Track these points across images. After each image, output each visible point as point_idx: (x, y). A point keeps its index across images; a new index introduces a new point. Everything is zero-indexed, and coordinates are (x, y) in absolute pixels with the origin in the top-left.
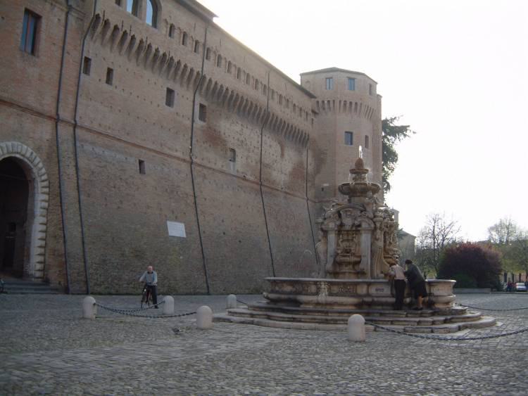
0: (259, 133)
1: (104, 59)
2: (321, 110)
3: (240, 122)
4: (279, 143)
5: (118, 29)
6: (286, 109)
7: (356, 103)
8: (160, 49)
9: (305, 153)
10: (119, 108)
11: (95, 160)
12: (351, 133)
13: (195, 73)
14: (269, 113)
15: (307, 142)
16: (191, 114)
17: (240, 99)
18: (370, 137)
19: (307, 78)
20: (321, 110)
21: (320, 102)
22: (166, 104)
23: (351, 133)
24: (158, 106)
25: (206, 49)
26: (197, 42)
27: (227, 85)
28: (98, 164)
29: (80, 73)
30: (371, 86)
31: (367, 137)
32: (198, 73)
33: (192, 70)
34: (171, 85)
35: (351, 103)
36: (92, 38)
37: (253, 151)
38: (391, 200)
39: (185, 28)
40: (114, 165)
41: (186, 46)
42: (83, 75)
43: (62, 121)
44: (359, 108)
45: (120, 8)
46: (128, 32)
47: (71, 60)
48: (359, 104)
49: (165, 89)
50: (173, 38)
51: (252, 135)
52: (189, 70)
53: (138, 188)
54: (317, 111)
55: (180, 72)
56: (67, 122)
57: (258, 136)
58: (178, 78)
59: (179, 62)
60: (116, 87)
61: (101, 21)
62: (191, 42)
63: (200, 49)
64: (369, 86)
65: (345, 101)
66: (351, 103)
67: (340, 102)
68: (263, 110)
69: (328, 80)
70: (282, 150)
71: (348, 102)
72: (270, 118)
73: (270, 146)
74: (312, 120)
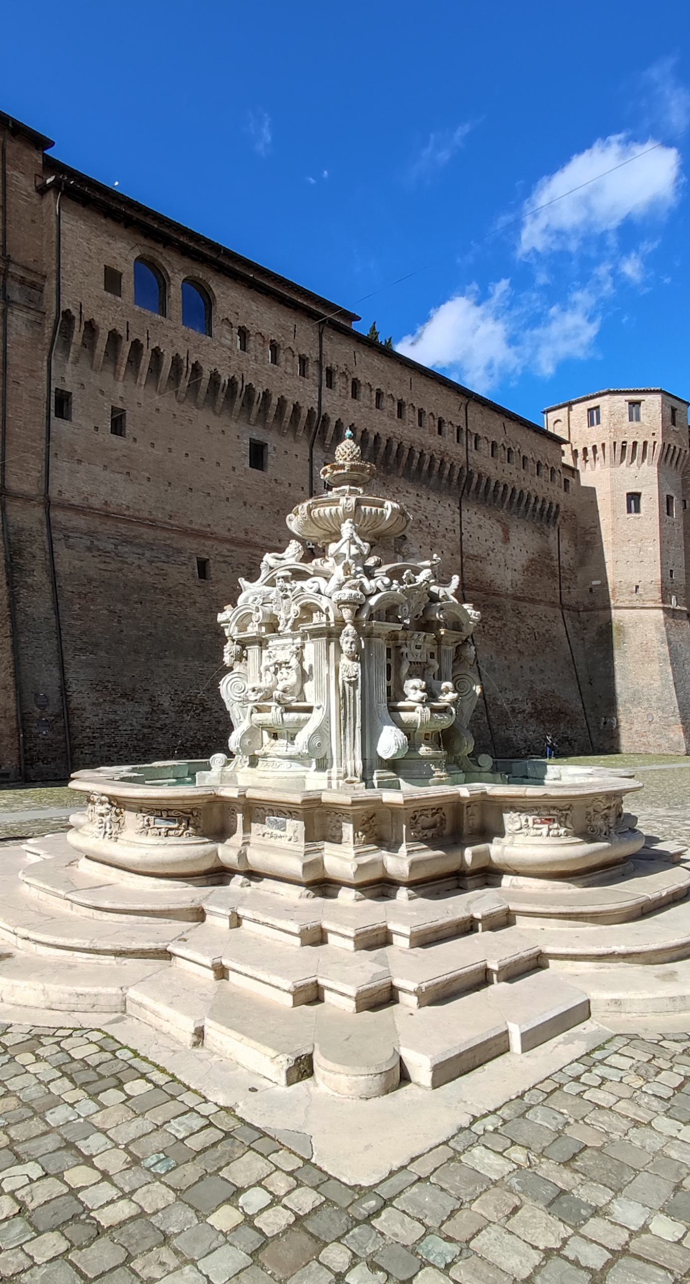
0: (455, 507)
1: (102, 392)
3: (411, 490)
4: (498, 521)
5: (121, 337)
6: (507, 464)
9: (553, 536)
10: (147, 475)
11: (96, 560)
13: (304, 413)
14: (470, 473)
15: (555, 517)
16: (307, 480)
17: (406, 453)
22: (250, 466)
24: (234, 469)
25: (324, 373)
26: (303, 360)
27: (376, 430)
28: (102, 566)
29: (48, 417)
32: (311, 411)
33: (297, 408)
34: (258, 434)
36: (68, 355)
37: (444, 536)
40: (139, 567)
42: (56, 422)
43: (16, 497)
45: (119, 299)
46: (143, 341)
47: (25, 396)
49: (247, 442)
51: (440, 510)
52: (290, 408)
53: (195, 603)
55: (272, 411)
56: (27, 499)
57: (454, 512)
58: (270, 420)
59: (266, 395)
60: (135, 440)
61: (77, 323)
62: (290, 357)
63: (312, 369)
67: (615, 443)
68: (457, 469)
70: (506, 531)
72: (475, 480)
73: (480, 526)
74: (566, 481)
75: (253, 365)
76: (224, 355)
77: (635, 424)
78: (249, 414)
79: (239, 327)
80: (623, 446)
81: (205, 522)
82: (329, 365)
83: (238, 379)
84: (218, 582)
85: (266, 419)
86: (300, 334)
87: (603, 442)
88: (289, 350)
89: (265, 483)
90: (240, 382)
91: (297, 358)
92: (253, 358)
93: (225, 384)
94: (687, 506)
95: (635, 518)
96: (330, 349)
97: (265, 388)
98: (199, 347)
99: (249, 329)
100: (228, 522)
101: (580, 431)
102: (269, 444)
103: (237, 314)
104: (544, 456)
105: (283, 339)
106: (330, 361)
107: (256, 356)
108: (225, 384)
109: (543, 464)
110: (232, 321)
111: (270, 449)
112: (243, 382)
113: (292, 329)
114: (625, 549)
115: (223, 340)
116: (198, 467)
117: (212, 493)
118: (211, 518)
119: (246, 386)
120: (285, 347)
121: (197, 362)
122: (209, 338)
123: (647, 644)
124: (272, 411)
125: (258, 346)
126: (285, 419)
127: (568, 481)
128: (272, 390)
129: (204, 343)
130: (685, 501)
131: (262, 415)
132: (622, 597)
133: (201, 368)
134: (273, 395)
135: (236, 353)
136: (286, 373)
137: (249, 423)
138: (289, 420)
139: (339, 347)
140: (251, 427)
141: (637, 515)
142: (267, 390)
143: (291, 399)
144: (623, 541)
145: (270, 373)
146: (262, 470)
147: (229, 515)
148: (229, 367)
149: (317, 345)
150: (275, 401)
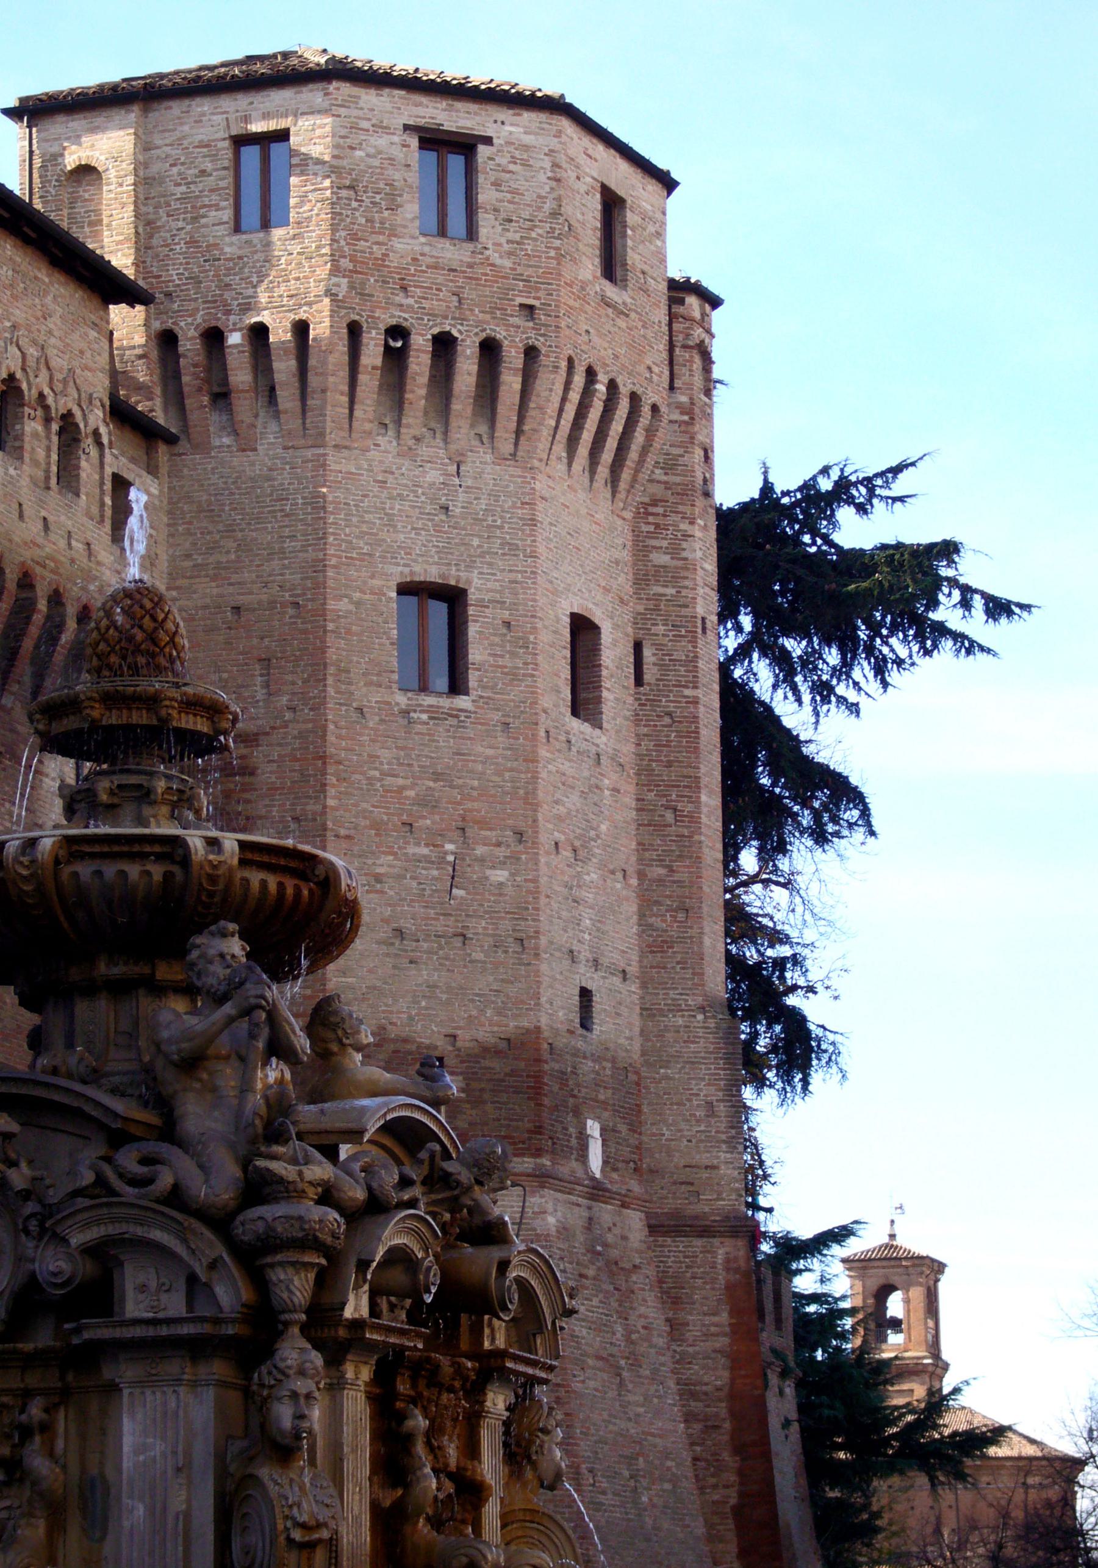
2: (198, 402)
7: (490, 349)
18: (609, 636)
20: (198, 402)
21: (190, 344)
35: (444, 345)
44: (511, 382)
48: (513, 357)
54: (159, 414)
64: (595, 203)
65: (397, 332)
66: (444, 345)
67: (354, 331)
71: (421, 343)
80: (387, 347)
94: (647, 677)
95: (435, 714)
101: (192, 242)
104: (32, 352)
109: (30, 394)
130: (638, 647)
141: (445, 702)
144: (378, 827)
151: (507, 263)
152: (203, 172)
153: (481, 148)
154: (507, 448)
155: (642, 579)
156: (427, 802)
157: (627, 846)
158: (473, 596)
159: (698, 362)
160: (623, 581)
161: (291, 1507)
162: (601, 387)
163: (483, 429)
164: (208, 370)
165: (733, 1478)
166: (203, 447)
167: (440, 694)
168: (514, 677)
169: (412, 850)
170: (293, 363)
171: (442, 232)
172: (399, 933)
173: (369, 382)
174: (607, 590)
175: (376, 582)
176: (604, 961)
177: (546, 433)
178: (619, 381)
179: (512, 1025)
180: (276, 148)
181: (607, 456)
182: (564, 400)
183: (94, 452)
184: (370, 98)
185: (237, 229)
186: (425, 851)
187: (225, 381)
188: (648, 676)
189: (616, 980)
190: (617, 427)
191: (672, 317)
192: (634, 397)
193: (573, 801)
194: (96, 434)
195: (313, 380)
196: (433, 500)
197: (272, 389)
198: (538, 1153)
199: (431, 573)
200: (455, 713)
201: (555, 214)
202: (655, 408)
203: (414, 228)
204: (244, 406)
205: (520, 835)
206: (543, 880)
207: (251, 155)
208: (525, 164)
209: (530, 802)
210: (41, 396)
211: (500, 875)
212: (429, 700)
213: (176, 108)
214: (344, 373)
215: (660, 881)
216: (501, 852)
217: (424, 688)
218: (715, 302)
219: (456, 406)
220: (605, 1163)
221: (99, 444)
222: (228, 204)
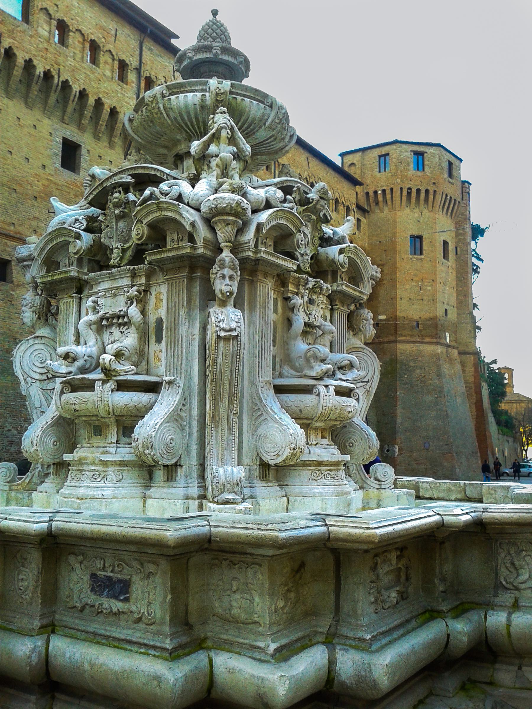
2: (373, 204)
7: (427, 191)
8: (35, 62)
12: (420, 238)
19: (349, 159)
21: (371, 194)
22: (62, 166)
23: (420, 238)
26: (123, 66)
30: (450, 164)
31: (445, 243)
35: (418, 191)
38: (245, 79)
39: (95, 35)
41: (98, 66)
44: (431, 197)
48: (431, 192)
50: (67, 47)
55: (88, 113)
58: (85, 122)
59: (83, 94)
62: (110, 61)
63: (132, 76)
65: (410, 189)
66: (418, 191)
69: (382, 159)
71: (414, 190)
75: (71, 62)
76: (41, 46)
77: (419, 173)
78: (64, 112)
79: (59, 19)
80: (408, 192)
81: (9, 220)
82: (148, 75)
83: (54, 73)
84: (18, 286)
85: (80, 120)
86: (121, 37)
87: (392, 186)
88: (108, 53)
89: (76, 186)
90: (56, 77)
91: (116, 63)
92: (72, 54)
93: (39, 76)
95: (417, 259)
96: (150, 60)
97: (82, 87)
98: (13, 33)
99: (69, 24)
100: (34, 223)
101: (372, 175)
102: (83, 145)
103: (57, 5)
104: (341, 194)
105: (103, 40)
106: (148, 70)
107: (74, 53)
108: (39, 76)
109: (340, 201)
110: (51, 12)
111: (84, 151)
112: (59, 77)
113: (113, 32)
114: (407, 287)
115: (40, 30)
116: (5, 159)
117: (18, 189)
118: (15, 216)
119: (63, 82)
120: (105, 50)
121: (10, 47)
122: (26, 25)
123: (425, 376)
124: (88, 113)
125: (77, 43)
126: (101, 122)
127: (360, 220)
128: (89, 90)
129: (19, 29)
130: (456, 248)
131: (77, 115)
132: (404, 332)
133: (14, 54)
134: (90, 96)
135: (53, 45)
136: (105, 75)
137: (63, 120)
138: (105, 124)
139: (159, 59)
140: (65, 125)
141: (419, 257)
142: (84, 89)
143: (108, 103)
144: (406, 280)
145: (88, 73)
146: (74, 172)
147: (37, 215)
148: (46, 59)
149: (137, 53)
150: (91, 101)
151: (430, 175)
152: (374, 163)
153: (425, 154)
154: (431, 209)
155: (457, 235)
156: (415, 275)
157: (454, 283)
158: (424, 237)
159: (467, 195)
160: (453, 234)
161: (219, 322)
162: (449, 198)
163: (426, 206)
164: (375, 199)
165: (474, 398)
166: (374, 212)
167: (418, 255)
168: (432, 251)
169: (413, 284)
170: (390, 196)
171: (418, 170)
172: (410, 299)
173: (404, 198)
174: (450, 236)
175: (406, 235)
176: (450, 304)
177: (438, 206)
178: (452, 197)
179: (431, 315)
180: (387, 157)
181: (450, 211)
182: (441, 200)
183: (353, 213)
184: (404, 146)
185: (380, 172)
186: (415, 284)
187: (378, 201)
188: (459, 253)
189: (452, 308)
190: (452, 205)
191: (462, 187)
192: (455, 200)
193: (443, 275)
194: (353, 210)
195: (394, 199)
196: (417, 220)
197: (386, 201)
198: (437, 339)
199: (416, 233)
200: (421, 259)
201: (439, 165)
202: (459, 202)
203: (412, 169)
204: (381, 204)
205: (433, 281)
206: (438, 289)
207: (382, 159)
208: (434, 157)
209: (435, 274)
210: (343, 202)
211: (429, 288)
212: (416, 256)
213: (369, 151)
214: (400, 197)
215: (461, 291)
216: (429, 284)
217: (415, 254)
218: (470, 184)
219: (421, 202)
220: (450, 340)
221: (354, 212)
222: (378, 168)
